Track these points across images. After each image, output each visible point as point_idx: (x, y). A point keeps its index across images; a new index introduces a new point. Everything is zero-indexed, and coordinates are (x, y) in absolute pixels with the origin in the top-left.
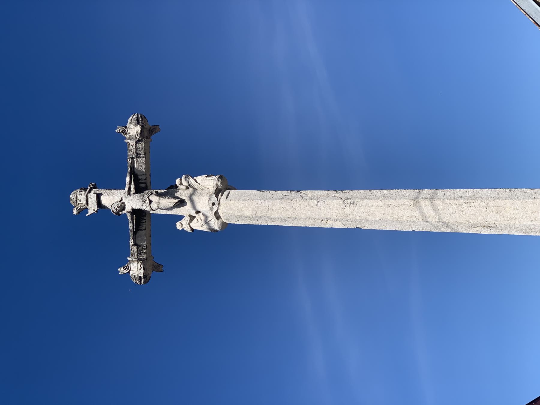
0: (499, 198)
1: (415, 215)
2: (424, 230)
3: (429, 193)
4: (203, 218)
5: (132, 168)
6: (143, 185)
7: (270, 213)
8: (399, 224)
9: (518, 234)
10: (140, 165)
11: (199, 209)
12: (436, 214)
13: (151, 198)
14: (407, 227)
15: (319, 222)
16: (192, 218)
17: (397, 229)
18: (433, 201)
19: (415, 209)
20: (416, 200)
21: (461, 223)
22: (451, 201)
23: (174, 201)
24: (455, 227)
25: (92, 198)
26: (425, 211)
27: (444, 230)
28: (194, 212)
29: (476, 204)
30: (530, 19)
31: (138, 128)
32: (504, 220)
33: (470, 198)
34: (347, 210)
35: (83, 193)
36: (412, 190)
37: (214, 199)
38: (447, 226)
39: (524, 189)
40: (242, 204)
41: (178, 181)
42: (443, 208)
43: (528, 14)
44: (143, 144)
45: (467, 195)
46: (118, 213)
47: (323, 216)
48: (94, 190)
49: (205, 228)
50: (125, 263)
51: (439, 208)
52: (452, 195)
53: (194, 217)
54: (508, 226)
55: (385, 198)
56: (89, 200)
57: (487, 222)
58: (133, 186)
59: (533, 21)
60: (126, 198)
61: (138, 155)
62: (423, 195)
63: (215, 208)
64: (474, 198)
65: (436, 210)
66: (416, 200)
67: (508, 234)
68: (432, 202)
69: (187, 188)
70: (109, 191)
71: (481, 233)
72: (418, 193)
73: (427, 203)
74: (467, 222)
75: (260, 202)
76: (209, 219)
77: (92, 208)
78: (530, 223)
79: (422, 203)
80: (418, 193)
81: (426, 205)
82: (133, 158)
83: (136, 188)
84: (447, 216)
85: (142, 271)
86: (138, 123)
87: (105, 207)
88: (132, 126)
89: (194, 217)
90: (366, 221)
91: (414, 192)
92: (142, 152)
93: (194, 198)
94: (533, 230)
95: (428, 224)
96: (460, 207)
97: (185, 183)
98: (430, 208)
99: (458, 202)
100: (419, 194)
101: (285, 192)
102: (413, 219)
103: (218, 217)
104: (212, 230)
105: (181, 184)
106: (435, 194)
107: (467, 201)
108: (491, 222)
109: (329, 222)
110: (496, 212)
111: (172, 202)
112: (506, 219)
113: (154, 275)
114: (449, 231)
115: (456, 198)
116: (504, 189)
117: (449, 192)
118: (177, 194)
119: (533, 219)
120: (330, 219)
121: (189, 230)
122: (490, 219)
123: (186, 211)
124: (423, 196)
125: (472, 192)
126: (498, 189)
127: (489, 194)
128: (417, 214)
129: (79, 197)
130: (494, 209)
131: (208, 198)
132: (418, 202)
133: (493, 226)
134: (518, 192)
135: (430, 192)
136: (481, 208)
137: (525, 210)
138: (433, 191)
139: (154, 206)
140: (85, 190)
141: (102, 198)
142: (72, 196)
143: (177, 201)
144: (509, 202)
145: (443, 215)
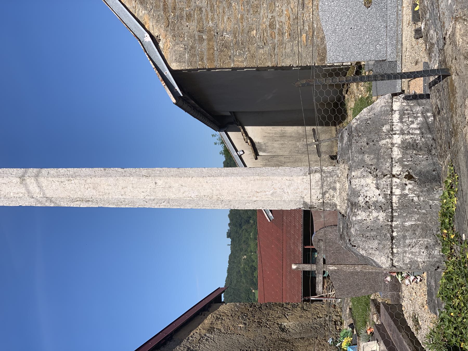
0: (95, 176)
1: (22, 191)
2: (29, 205)
3: (35, 171)
8: (6, 200)
9: (111, 207)
12: (40, 191)
14: (14, 202)
17: (5, 205)
18: (38, 179)
19: (22, 186)
20: (22, 178)
21: (63, 198)
22: (54, 179)
24: (58, 202)
26: (31, 188)
27: (48, 204)
29: (76, 181)
30: (131, 32)
32: (100, 195)
33: (71, 176)
36: (19, 169)
39: (116, 169)
42: (47, 185)
43: (130, 28)
45: (69, 173)
51: (43, 185)
52: (56, 174)
54: (103, 199)
57: (85, 197)
59: (133, 34)
62: (29, 173)
64: (74, 176)
65: (40, 187)
66: (22, 178)
67: (103, 206)
68: (37, 180)
71: (81, 206)
72: (24, 172)
73: (33, 181)
74: (68, 197)
78: (121, 197)
79: (28, 181)
80: (24, 172)
81: (31, 183)
84: (51, 192)
91: (20, 171)
94: (123, 203)
95: (33, 199)
96: (62, 184)
98: (35, 185)
99: (60, 180)
102: (19, 195)
107: (68, 179)
108: (89, 197)
110: (93, 188)
112: (101, 193)
114: (52, 205)
115: (58, 176)
116: (100, 168)
117: (53, 171)
119: (123, 193)
122: (89, 193)
124: (29, 174)
125: (73, 171)
126: (95, 169)
127: (87, 173)
128: (23, 190)
130: (91, 186)
132: (24, 180)
133: (90, 200)
134: (111, 171)
135: (35, 170)
136: (80, 185)
137: (117, 186)
144: (104, 179)
145: (46, 192)
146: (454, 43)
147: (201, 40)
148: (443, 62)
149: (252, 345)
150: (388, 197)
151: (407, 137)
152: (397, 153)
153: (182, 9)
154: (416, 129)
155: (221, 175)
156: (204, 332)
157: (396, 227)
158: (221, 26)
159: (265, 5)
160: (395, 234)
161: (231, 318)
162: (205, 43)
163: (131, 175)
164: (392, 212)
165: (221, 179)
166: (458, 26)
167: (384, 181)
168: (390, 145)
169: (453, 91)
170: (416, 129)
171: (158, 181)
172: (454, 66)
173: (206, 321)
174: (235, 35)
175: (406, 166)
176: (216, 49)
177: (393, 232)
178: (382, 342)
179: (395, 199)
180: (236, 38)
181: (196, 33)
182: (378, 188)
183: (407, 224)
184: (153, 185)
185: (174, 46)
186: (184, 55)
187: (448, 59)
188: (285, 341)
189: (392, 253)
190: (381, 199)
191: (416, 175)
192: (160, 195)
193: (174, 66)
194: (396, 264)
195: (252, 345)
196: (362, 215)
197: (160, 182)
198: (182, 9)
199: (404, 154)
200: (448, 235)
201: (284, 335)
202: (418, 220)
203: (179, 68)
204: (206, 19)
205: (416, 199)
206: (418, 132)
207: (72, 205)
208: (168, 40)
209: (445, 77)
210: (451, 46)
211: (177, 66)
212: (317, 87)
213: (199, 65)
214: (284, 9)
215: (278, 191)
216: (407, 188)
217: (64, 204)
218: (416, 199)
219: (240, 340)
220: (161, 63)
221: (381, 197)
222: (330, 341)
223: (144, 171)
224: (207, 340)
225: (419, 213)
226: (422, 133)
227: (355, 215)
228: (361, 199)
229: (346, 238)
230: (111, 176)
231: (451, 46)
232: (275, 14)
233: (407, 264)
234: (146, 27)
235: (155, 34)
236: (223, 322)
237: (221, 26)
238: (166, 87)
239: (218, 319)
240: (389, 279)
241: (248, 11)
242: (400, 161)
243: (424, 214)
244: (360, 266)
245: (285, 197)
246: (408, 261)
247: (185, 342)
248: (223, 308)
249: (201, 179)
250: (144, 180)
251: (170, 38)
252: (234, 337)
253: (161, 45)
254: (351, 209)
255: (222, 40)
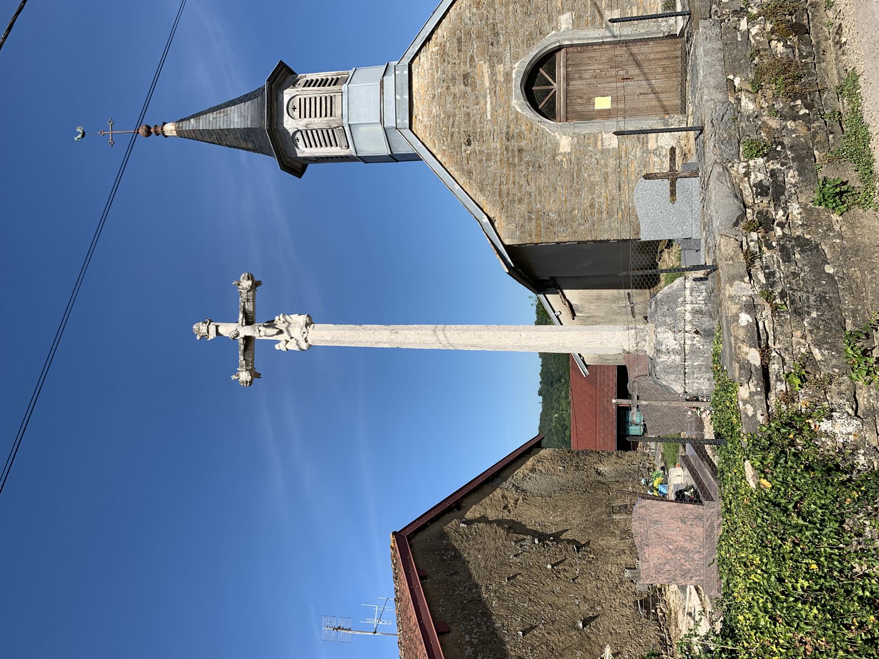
4: (295, 342)
5: (244, 308)
6: (251, 320)
7: (343, 338)
10: (249, 307)
11: (293, 336)
13: (260, 328)
15: (374, 343)
16: (287, 342)
23: (275, 331)
25: (212, 328)
26: (440, 337)
27: (450, 348)
28: (289, 337)
31: (250, 283)
34: (393, 337)
35: (204, 325)
37: (304, 330)
38: (452, 346)
40: (324, 333)
41: (277, 318)
44: (251, 293)
46: (234, 339)
47: (377, 340)
48: (212, 323)
49: (296, 348)
50: (236, 372)
53: (288, 341)
55: (416, 330)
56: (210, 330)
58: (244, 321)
60: (240, 328)
61: (248, 300)
63: (305, 335)
65: (446, 337)
66: (434, 331)
69: (284, 322)
70: (224, 324)
75: (336, 331)
76: (299, 343)
77: (212, 335)
82: (244, 302)
83: (246, 322)
85: (250, 377)
86: (249, 279)
87: (221, 335)
88: (245, 281)
89: (288, 341)
90: (404, 343)
92: (251, 298)
93: (290, 329)
97: (282, 319)
98: (442, 335)
99: (458, 332)
100: (436, 327)
101: (352, 326)
103: (306, 341)
104: (302, 350)
105: (279, 320)
106: (445, 327)
109: (381, 344)
111: (275, 331)
113: (255, 379)
114: (452, 349)
115: (457, 330)
117: (453, 327)
118: (276, 326)
120: (381, 342)
121: (285, 350)
122: (476, 341)
123: (284, 336)
128: (435, 339)
129: (201, 328)
131: (300, 329)
135: (442, 326)
138: (444, 326)
139: (262, 334)
140: (206, 323)
141: (219, 328)
142: (195, 327)
143: (278, 330)
145: (449, 340)
146: (720, 249)
147: (530, 219)
148: (714, 260)
149: (570, 484)
150: (682, 346)
151: (696, 306)
152: (688, 317)
153: (514, 195)
154: (701, 300)
155: (565, 331)
156: (526, 472)
157: (688, 366)
158: (548, 208)
159: (586, 189)
160: (686, 371)
161: (551, 461)
162: (534, 222)
163: (504, 330)
164: (685, 356)
165: (565, 333)
166: (722, 240)
167: (680, 335)
168: (683, 311)
169: (720, 279)
170: (701, 300)
171: (522, 334)
172: (722, 264)
173: (528, 463)
174: (560, 215)
175: (695, 325)
176: (542, 227)
177: (685, 369)
178: (686, 468)
179: (687, 347)
180: (560, 217)
181: (526, 214)
182: (675, 340)
183: (696, 364)
184: (519, 336)
185: (507, 225)
186: (515, 232)
187: (717, 259)
188: (601, 483)
189: (685, 383)
190: (677, 347)
191: (702, 331)
192: (523, 343)
193: (507, 242)
194: (687, 390)
195: (570, 484)
196: (664, 358)
197: (523, 335)
198: (514, 195)
199: (693, 317)
200: (717, 368)
201: (600, 478)
202: (703, 361)
203: (511, 243)
204: (535, 202)
205: (701, 347)
206: (703, 302)
207: (465, 349)
208: (502, 221)
209: (714, 270)
210: (718, 252)
211: (509, 242)
212: (634, 276)
213: (528, 240)
214: (603, 191)
215: (605, 341)
216: (695, 340)
217: (459, 348)
218: (701, 347)
219: (560, 480)
220: (496, 240)
221: (677, 345)
222: (643, 481)
223: (512, 327)
224: (529, 479)
225: (703, 357)
226: (706, 303)
227: (659, 358)
228: (663, 347)
229: (654, 374)
230: (491, 330)
231: (718, 252)
232: (594, 196)
233: (694, 391)
234: (484, 210)
235: (492, 216)
236: (544, 464)
237: (548, 208)
238: (500, 259)
239: (539, 461)
240: (690, 413)
241: (571, 194)
242: (691, 322)
243: (707, 357)
244: (667, 402)
245: (610, 346)
246: (695, 388)
247: (510, 479)
248: (543, 452)
249: (551, 333)
250: (513, 333)
251: (504, 218)
252: (554, 477)
253: (496, 224)
254: (657, 354)
255: (548, 219)
